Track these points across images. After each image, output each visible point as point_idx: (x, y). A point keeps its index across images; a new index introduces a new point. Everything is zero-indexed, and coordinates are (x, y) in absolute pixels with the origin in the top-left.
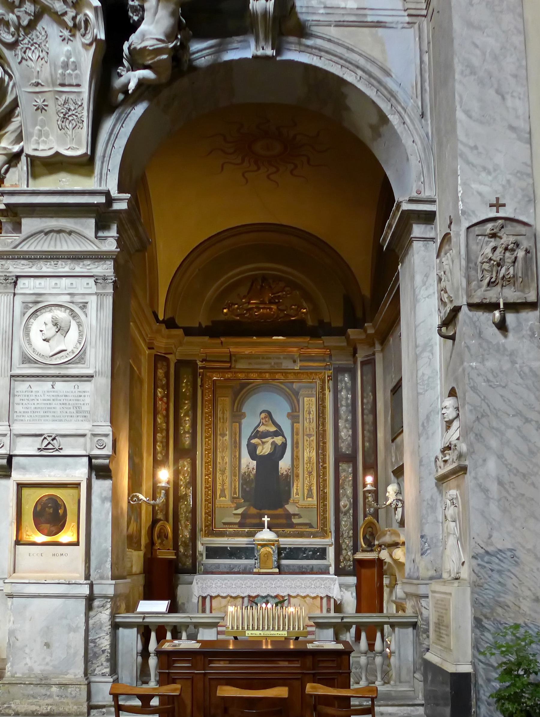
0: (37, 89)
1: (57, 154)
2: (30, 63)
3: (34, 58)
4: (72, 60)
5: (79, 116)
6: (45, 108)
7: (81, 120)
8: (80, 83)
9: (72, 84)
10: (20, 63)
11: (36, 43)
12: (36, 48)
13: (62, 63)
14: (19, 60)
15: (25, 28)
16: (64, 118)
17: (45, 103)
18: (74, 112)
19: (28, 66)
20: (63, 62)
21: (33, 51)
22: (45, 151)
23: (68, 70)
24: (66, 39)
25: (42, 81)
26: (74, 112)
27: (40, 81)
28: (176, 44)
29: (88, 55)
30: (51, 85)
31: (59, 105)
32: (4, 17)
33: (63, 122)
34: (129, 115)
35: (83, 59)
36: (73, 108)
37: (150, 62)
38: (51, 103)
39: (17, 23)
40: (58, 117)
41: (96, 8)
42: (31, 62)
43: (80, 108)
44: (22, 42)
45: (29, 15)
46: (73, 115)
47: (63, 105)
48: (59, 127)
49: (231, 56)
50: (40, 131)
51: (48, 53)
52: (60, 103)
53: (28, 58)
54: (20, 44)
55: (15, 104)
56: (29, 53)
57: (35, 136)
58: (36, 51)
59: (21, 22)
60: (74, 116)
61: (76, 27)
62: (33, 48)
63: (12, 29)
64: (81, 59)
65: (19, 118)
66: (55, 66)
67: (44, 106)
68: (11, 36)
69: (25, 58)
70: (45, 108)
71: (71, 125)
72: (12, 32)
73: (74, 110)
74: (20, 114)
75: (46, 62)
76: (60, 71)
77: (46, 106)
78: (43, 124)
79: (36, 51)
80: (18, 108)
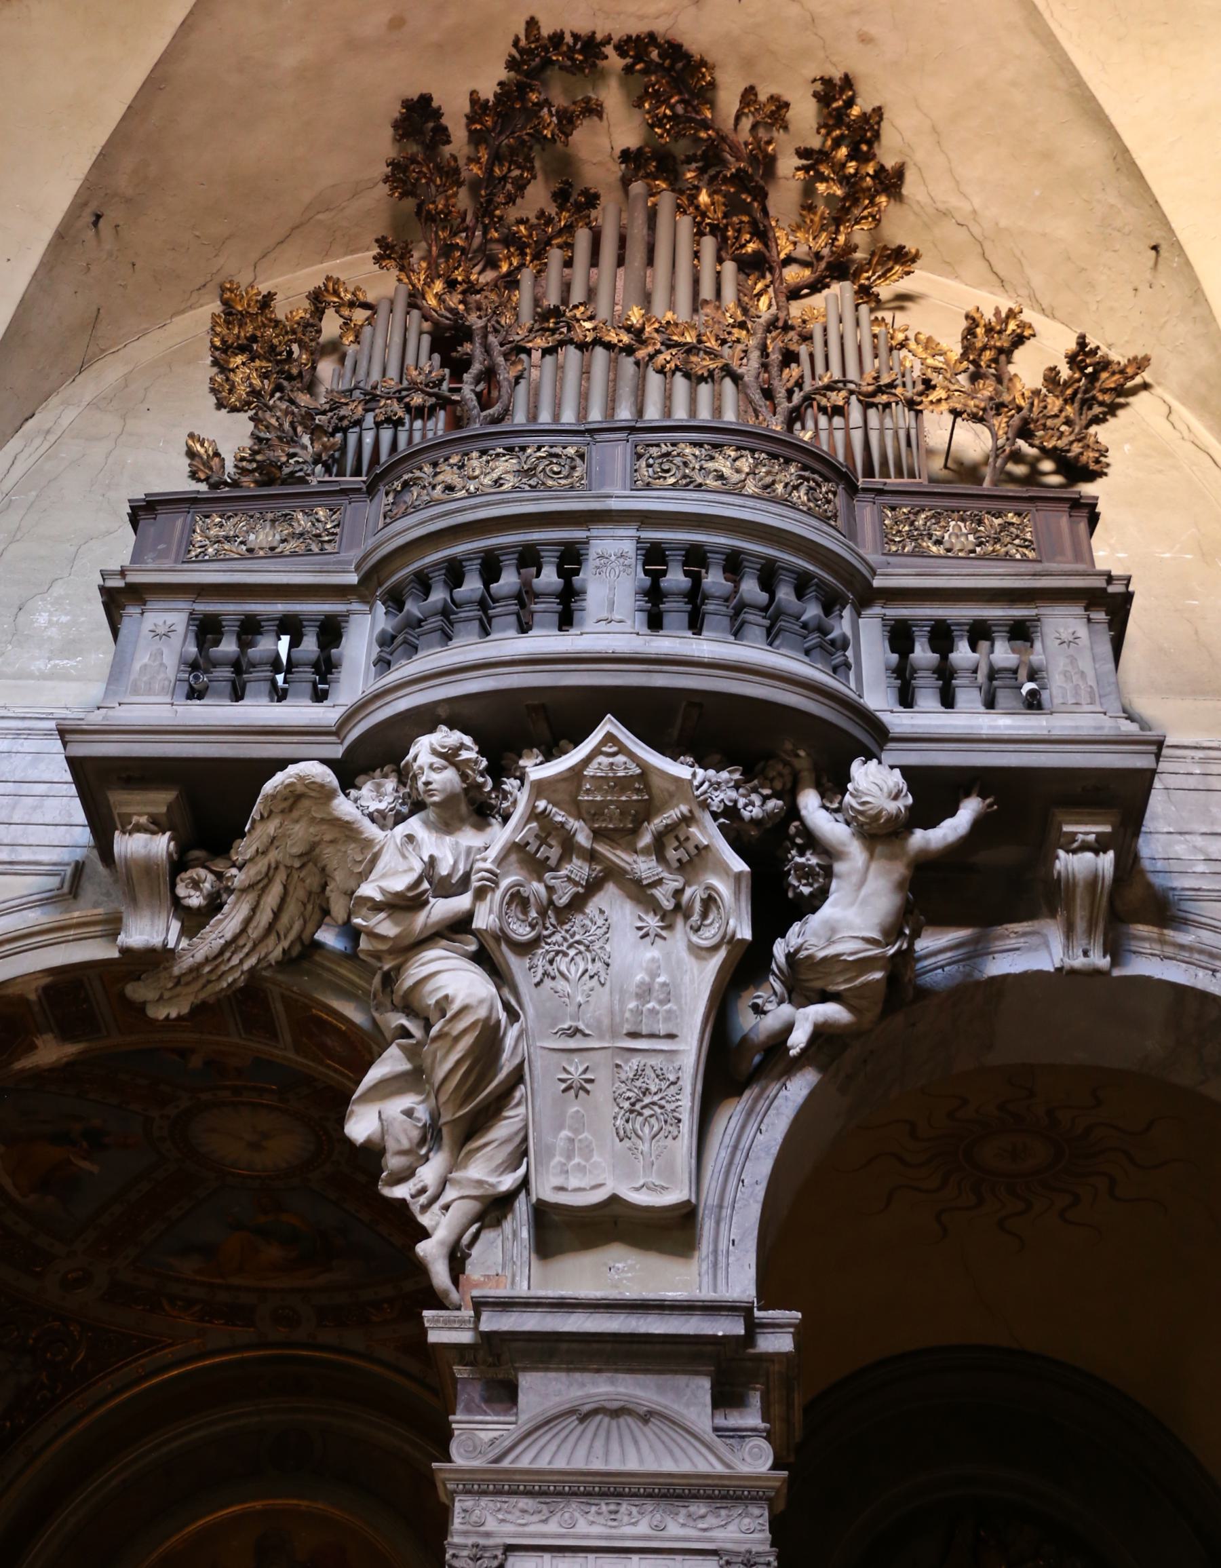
0: (572, 1044)
2: (561, 984)
3: (574, 973)
4: (661, 979)
8: (674, 1032)
10: (538, 984)
12: (580, 952)
13: (638, 986)
14: (537, 979)
15: (559, 911)
19: (556, 992)
20: (642, 983)
21: (572, 959)
22: (584, 1193)
23: (649, 1002)
24: (652, 936)
25: (587, 1026)
27: (582, 1026)
28: (900, 947)
29: (701, 972)
30: (607, 1037)
31: (623, 1082)
35: (687, 978)
37: (843, 987)
38: (602, 1076)
39: (545, 902)
41: (738, 876)
43: (673, 1089)
44: (549, 941)
45: (576, 884)
47: (633, 1080)
49: (1000, 966)
53: (557, 974)
55: (517, 1076)
56: (562, 963)
58: (578, 959)
59: (554, 897)
61: (681, 909)
62: (572, 952)
63: (533, 914)
64: (682, 979)
66: (622, 992)
68: (528, 929)
69: (552, 974)
72: (534, 919)
74: (524, 1100)
75: (603, 985)
76: (632, 1005)
78: (579, 1124)
79: (578, 959)
80: (522, 1087)
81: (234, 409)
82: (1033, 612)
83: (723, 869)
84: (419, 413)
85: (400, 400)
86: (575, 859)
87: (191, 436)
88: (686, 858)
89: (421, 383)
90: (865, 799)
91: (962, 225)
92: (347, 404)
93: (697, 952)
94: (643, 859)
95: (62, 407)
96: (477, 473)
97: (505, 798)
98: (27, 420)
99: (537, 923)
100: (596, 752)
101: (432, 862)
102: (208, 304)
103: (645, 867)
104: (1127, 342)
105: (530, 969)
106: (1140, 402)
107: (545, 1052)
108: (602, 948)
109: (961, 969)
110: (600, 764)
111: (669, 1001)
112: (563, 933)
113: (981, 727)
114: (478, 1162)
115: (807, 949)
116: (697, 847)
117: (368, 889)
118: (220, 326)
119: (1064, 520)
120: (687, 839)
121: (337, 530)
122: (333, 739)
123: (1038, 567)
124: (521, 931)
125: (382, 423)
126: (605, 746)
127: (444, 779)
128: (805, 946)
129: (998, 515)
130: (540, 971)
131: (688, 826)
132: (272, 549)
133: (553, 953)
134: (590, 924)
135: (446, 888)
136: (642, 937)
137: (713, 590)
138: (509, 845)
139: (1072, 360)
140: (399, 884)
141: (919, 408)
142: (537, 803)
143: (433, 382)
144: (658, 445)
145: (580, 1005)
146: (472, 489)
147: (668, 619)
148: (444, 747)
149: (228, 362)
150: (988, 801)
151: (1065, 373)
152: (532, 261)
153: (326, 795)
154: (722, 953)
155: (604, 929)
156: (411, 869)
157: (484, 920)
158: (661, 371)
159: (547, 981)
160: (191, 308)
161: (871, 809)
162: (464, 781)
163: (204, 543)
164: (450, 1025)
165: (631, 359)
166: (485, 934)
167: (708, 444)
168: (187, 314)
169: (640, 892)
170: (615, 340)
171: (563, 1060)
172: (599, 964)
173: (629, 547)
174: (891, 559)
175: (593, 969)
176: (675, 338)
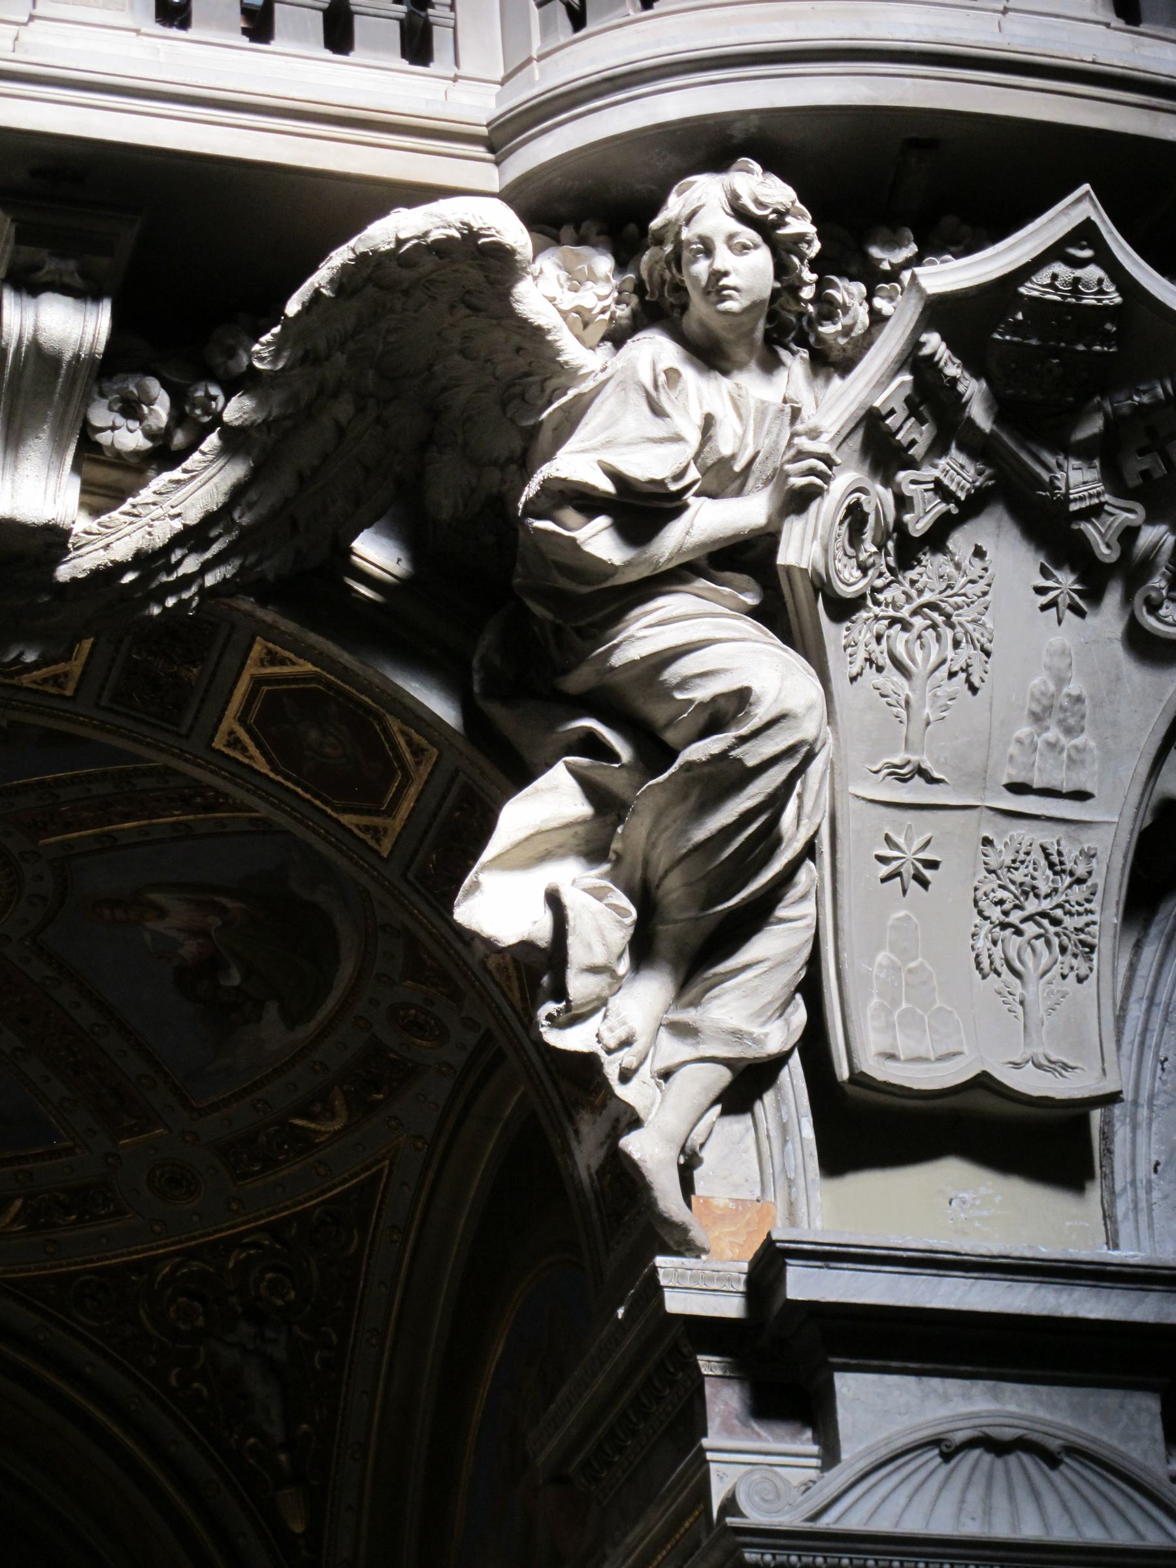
1: (983, 1082)
2: (892, 679)
4: (1073, 688)
5: (1068, 922)
6: (928, 873)
7: (1083, 943)
8: (1089, 788)
9: (1058, 788)
10: (853, 679)
11: (933, 606)
12: (934, 626)
14: (855, 670)
16: (1004, 926)
17: (925, 855)
18: (1046, 905)
21: (920, 637)
23: (1047, 729)
25: (936, 762)
27: (927, 765)
33: (995, 943)
36: (1044, 889)
40: (978, 920)
42: (897, 677)
44: (881, 597)
46: (1043, 914)
51: (988, 654)
52: (994, 863)
54: (869, 602)
57: (875, 991)
59: (907, 518)
60: (1045, 922)
62: (918, 622)
67: (919, 866)
68: (858, 574)
69: (881, 662)
70: (928, 873)
71: (1028, 955)
73: (1046, 897)
75: (974, 690)
77: (933, 865)
86: (954, 451)
94: (1075, 463)
97: (831, 317)
99: (873, 565)
101: (709, 422)
105: (845, 648)
108: (975, 621)
110: (1055, 277)
111: (1082, 730)
114: (726, 998)
122: (480, 151)
124: (846, 575)
126: (1073, 246)
130: (862, 655)
133: (886, 622)
134: (955, 572)
136: (1044, 608)
138: (862, 413)
142: (924, 338)
145: (928, 724)
148: (760, 204)
155: (981, 586)
156: (677, 439)
159: (870, 673)
162: (778, 276)
166: (797, 577)
171: (891, 822)
172: (966, 650)
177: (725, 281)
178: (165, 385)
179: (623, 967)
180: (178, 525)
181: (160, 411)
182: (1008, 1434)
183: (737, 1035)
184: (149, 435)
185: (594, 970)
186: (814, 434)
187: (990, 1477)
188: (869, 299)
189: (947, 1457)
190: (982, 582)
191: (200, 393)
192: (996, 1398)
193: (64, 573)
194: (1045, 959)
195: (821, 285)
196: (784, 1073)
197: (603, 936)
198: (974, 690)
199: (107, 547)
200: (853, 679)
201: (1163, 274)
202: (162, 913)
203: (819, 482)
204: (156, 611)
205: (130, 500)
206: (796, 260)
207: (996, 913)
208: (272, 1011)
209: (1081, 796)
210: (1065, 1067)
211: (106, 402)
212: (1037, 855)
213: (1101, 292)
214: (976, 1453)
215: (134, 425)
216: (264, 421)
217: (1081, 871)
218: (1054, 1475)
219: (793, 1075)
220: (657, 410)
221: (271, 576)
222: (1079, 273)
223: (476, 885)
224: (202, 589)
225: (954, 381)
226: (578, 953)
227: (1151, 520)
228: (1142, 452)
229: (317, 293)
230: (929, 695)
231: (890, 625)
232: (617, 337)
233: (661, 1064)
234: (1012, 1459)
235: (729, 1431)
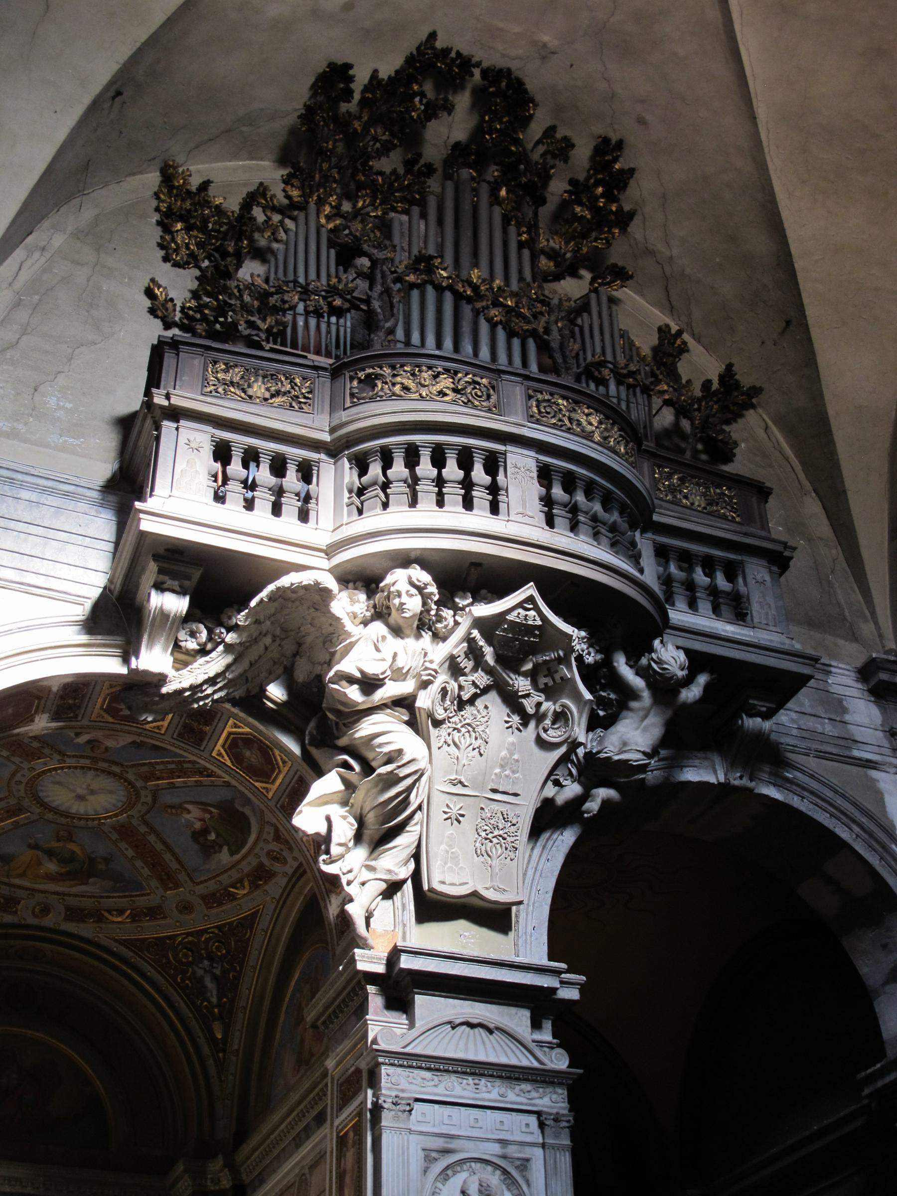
1: (475, 894)
2: (453, 749)
4: (516, 757)
5: (508, 838)
6: (461, 819)
7: (514, 847)
8: (519, 793)
10: (439, 748)
11: (469, 725)
12: (469, 732)
14: (440, 745)
16: (486, 839)
17: (461, 812)
18: (501, 832)
25: (466, 779)
26: (501, 832)
27: (463, 780)
32: (447, 685)
34: (556, 844)
36: (501, 826)
40: (477, 836)
44: (451, 720)
46: (500, 836)
48: (476, 852)
50: (447, 852)
51: (487, 743)
52: (484, 817)
59: (462, 693)
60: (501, 838)
62: (463, 730)
63: (448, 702)
65: (418, 828)
70: (461, 819)
71: (494, 850)
73: (502, 829)
75: (481, 755)
76: (497, 771)
77: (463, 816)
81: (176, 265)
82: (739, 558)
83: (577, 697)
84: (339, 312)
85: (324, 298)
87: (153, 280)
88: (551, 683)
89: (341, 290)
90: (666, 666)
91: (659, 264)
92: (288, 292)
93: (541, 743)
94: (523, 678)
95: (52, 231)
96: (426, 383)
97: (440, 621)
98: (28, 235)
100: (520, 605)
102: (151, 172)
103: (522, 684)
104: (745, 373)
106: (750, 415)
107: (441, 794)
108: (483, 731)
109: (662, 774)
112: (460, 717)
113: (717, 629)
115: (606, 753)
116: (562, 678)
117: (348, 665)
118: (164, 194)
119: (754, 499)
120: (557, 671)
121: (310, 396)
122: (323, 555)
123: (744, 529)
124: (439, 711)
125: (312, 312)
126: (526, 603)
127: (414, 604)
128: (605, 750)
129: (719, 486)
130: (443, 740)
131: (560, 664)
132: (266, 400)
135: (399, 675)
136: (508, 728)
137: (582, 506)
139: (721, 378)
140: (374, 668)
141: (652, 393)
142: (472, 631)
143: (349, 291)
144: (542, 393)
145: (464, 766)
146: (424, 394)
147: (558, 521)
148: (418, 581)
149: (172, 226)
150: (714, 676)
151: (715, 386)
152: (380, 204)
153: (325, 594)
154: (563, 749)
155: (486, 719)
157: (424, 701)
158: (489, 320)
159: (445, 746)
160: (141, 173)
161: (668, 673)
162: (423, 606)
163: (214, 383)
164: (400, 770)
165: (470, 307)
166: (422, 712)
167: (572, 400)
168: (136, 177)
169: (512, 701)
170: (462, 290)
172: (479, 741)
173: (532, 465)
174: (663, 504)
175: (476, 744)
176: (501, 300)
177: (404, 607)
178: (206, 627)
179: (351, 844)
180: (206, 677)
181: (204, 635)
182: (475, 1021)
183: (390, 871)
184: (199, 644)
185: (340, 845)
186: (431, 662)
187: (468, 1036)
188: (454, 616)
189: (453, 1028)
190: (486, 718)
191: (218, 631)
192: (472, 1008)
193: (164, 690)
194: (500, 852)
195: (437, 610)
196: (405, 886)
197: (345, 833)
198: (481, 755)
199: (180, 682)
200: (439, 748)
201: (556, 615)
202: (189, 812)
203: (432, 678)
204: (196, 706)
205: (190, 667)
206: (430, 601)
207: (483, 834)
208: (225, 849)
209: (516, 795)
210: (504, 890)
211: (184, 631)
212: (499, 815)
213: (535, 620)
214: (464, 1027)
215: (194, 640)
216: (240, 643)
217: (514, 822)
218: (491, 1037)
219: (408, 887)
220: (377, 649)
221: (237, 697)
222: (527, 613)
223: (301, 812)
224: (213, 700)
225: (482, 647)
226: (335, 838)
227: (547, 700)
228: (545, 676)
229: (262, 600)
230: (465, 756)
231: (454, 730)
232: (365, 623)
233: (362, 879)
234: (476, 1030)
235: (376, 1014)
